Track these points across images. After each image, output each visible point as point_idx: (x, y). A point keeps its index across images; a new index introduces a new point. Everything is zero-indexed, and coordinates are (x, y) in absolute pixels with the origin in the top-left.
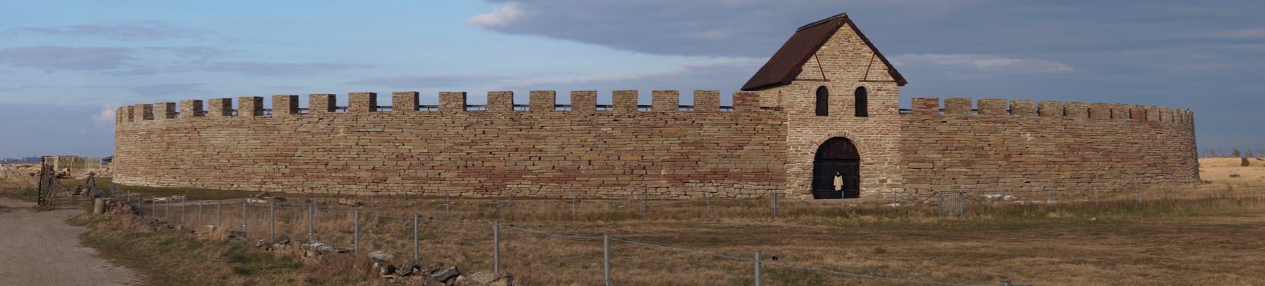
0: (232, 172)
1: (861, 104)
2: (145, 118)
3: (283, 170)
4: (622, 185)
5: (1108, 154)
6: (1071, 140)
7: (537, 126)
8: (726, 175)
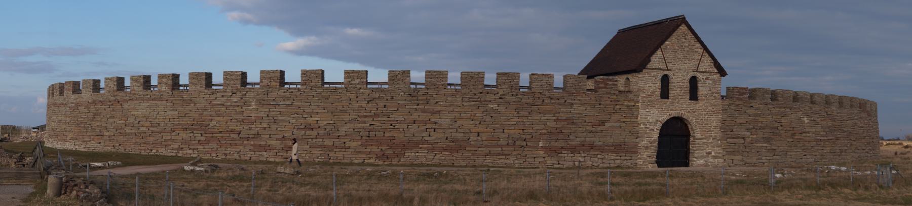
0: (151, 139)
2: (74, 93)
3: (199, 137)
4: (506, 155)
6: (830, 123)
7: (432, 102)
8: (592, 147)
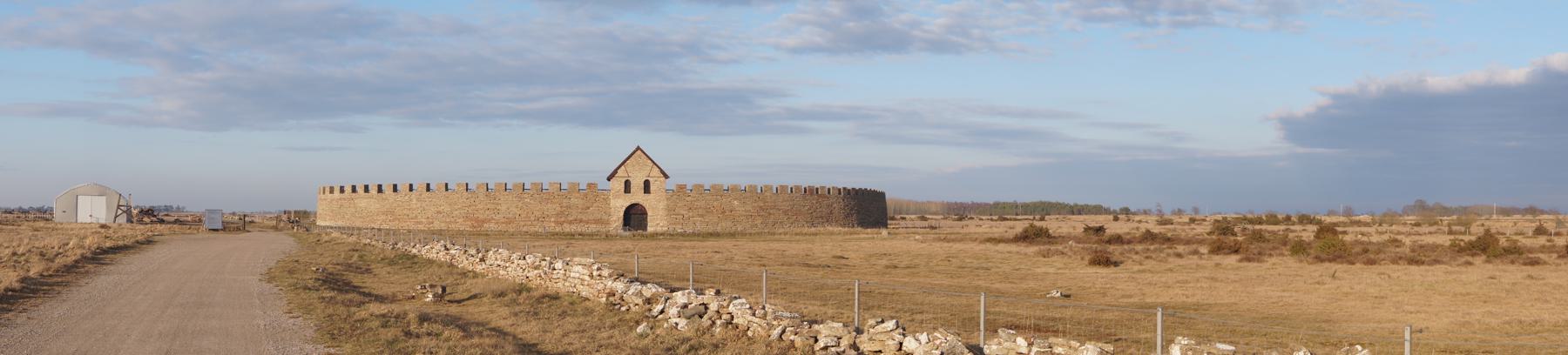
1: (647, 187)
5: (785, 212)
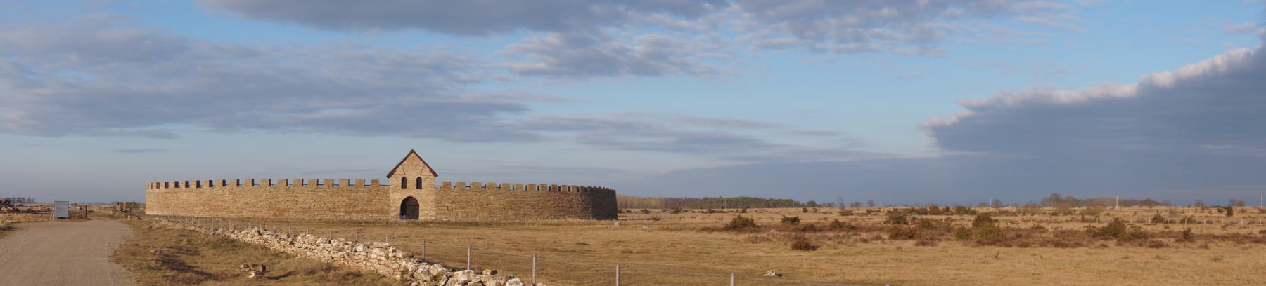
1: (419, 183)
5: (533, 206)
